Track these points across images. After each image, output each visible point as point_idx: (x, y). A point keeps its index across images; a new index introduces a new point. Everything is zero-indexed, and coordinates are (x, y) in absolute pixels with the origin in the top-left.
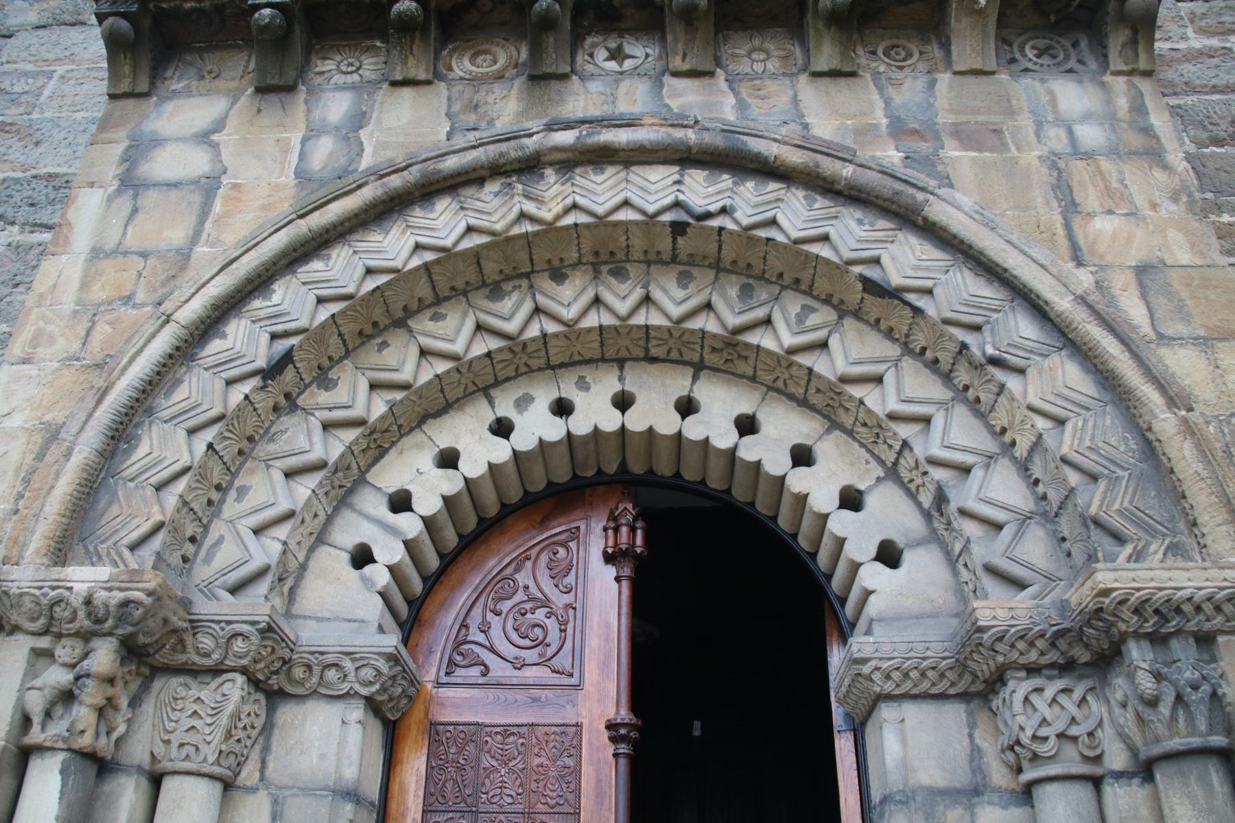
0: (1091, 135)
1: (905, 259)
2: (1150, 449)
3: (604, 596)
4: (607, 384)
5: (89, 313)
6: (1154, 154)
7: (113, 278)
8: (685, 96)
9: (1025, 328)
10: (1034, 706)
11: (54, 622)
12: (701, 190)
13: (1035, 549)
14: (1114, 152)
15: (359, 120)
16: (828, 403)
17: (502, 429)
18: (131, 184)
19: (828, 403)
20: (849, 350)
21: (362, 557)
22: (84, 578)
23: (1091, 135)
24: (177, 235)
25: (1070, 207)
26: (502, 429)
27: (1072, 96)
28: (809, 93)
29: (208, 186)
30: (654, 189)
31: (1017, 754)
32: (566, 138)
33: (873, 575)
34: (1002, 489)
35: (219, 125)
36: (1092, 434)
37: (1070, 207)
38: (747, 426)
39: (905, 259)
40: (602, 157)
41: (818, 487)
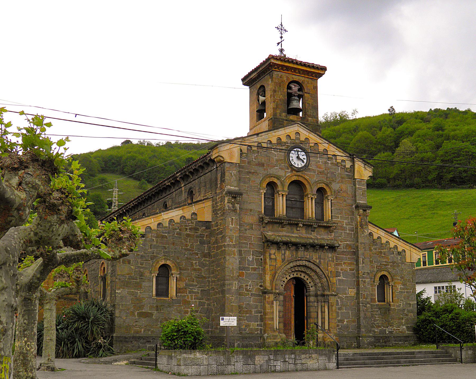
0: (330, 259)
1: (318, 270)
2: (328, 285)
3: (293, 287)
4: (296, 273)
5: (271, 270)
6: (334, 261)
7: (272, 267)
8: (306, 253)
9: (324, 276)
10: (320, 298)
11: (275, 293)
12: (307, 263)
13: (321, 289)
14: (331, 261)
15: (285, 254)
16: (310, 276)
17: (290, 276)
18: (270, 259)
19: (310, 276)
20: (312, 274)
21: (282, 285)
22: (277, 291)
23: (330, 259)
24: (275, 264)
25: (328, 266)
26: (290, 276)
27: (330, 255)
28: (314, 254)
29: (276, 259)
30: (304, 263)
31: (317, 300)
32: (300, 259)
33: (311, 288)
34: (320, 285)
35: (275, 253)
36: (326, 284)
37: (328, 266)
38: (304, 277)
39: (318, 270)
40: (300, 260)
41: (308, 282)
